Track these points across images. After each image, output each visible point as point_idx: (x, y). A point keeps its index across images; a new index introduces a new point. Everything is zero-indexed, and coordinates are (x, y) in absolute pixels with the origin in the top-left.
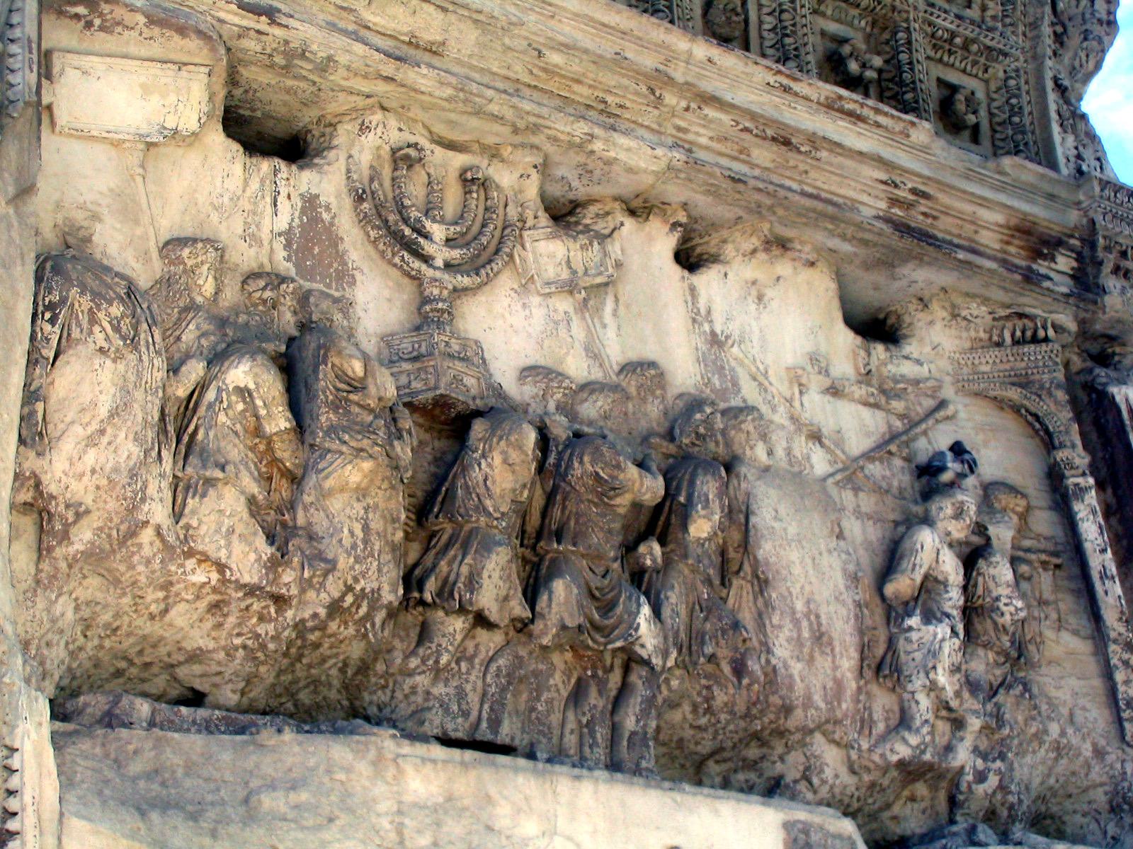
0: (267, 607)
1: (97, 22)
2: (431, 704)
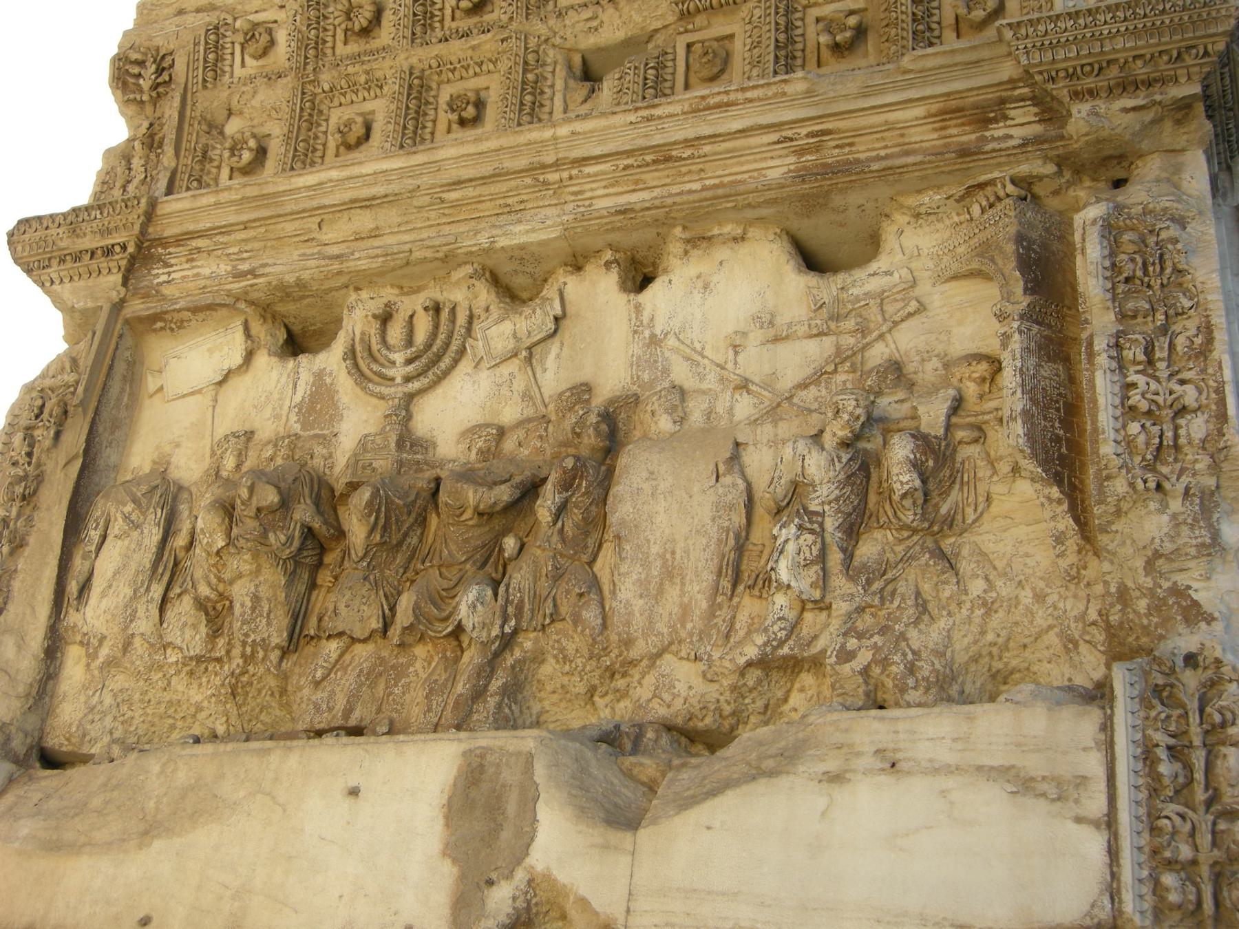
1: (173, 326)
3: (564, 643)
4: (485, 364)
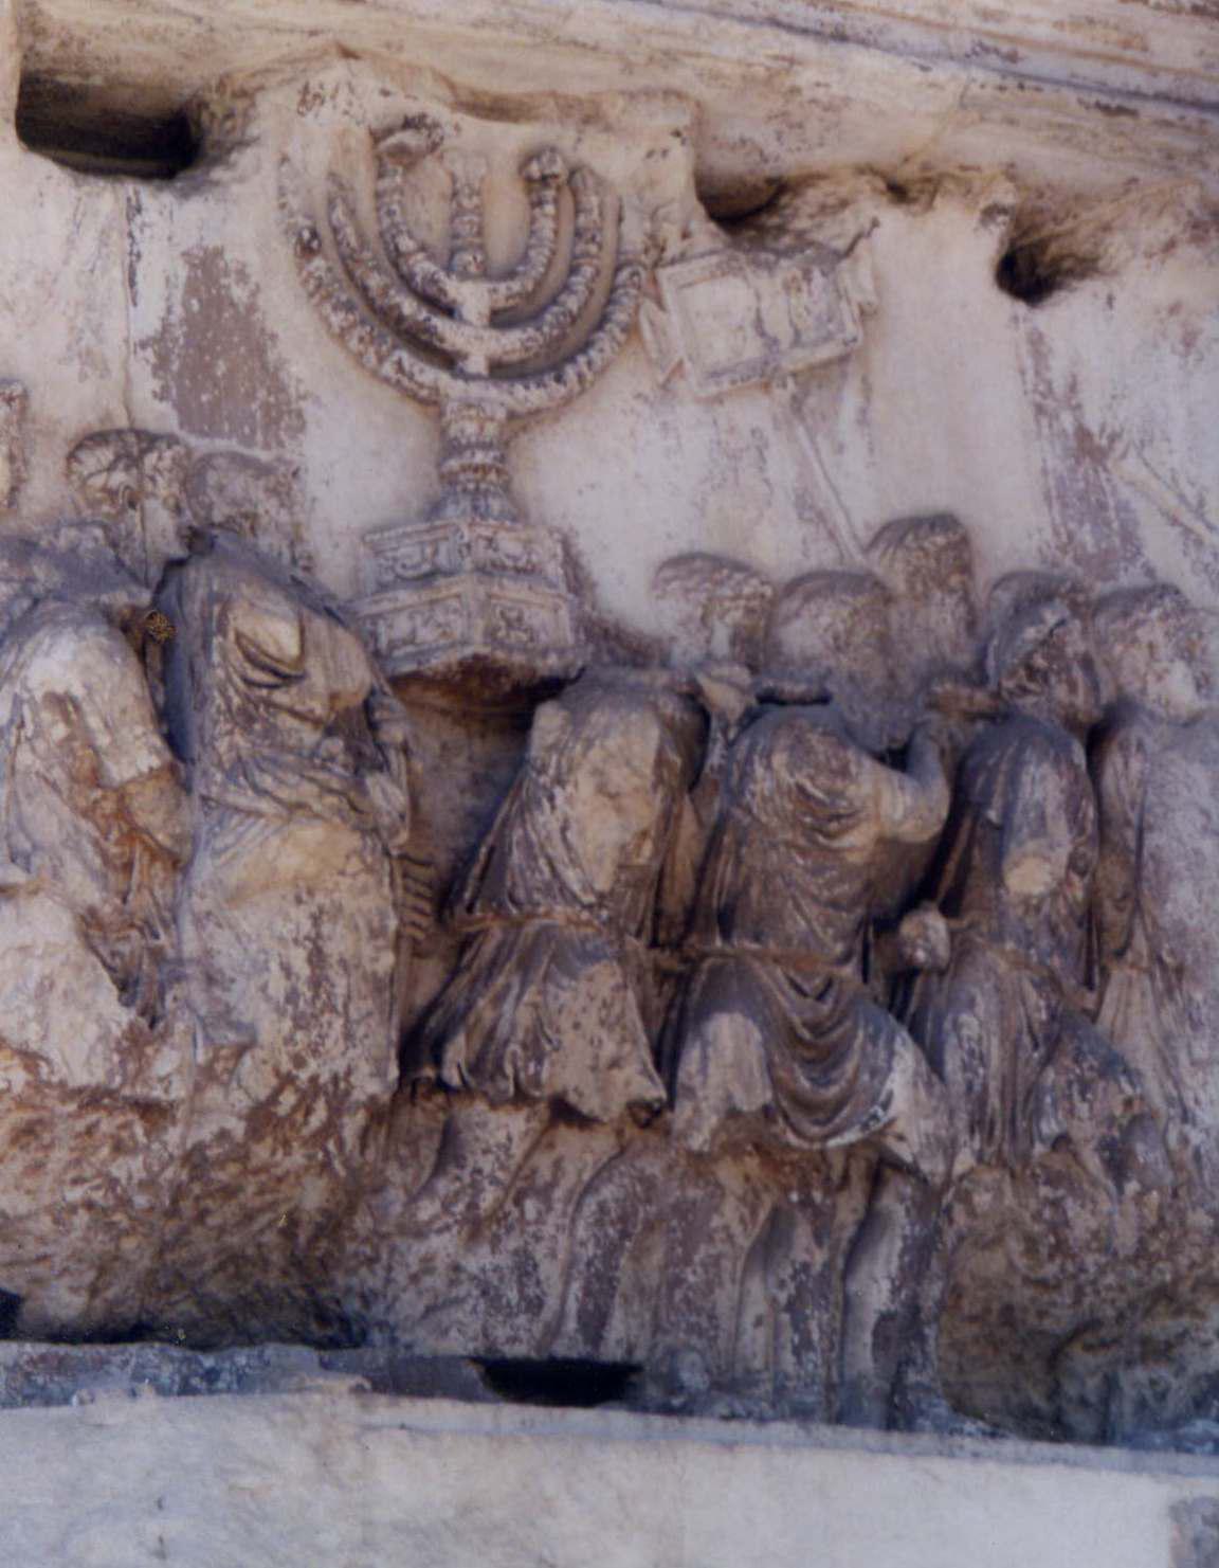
0: (126, 1126)
2: (462, 1291)
3: (1072, 1207)
4: (690, 384)
